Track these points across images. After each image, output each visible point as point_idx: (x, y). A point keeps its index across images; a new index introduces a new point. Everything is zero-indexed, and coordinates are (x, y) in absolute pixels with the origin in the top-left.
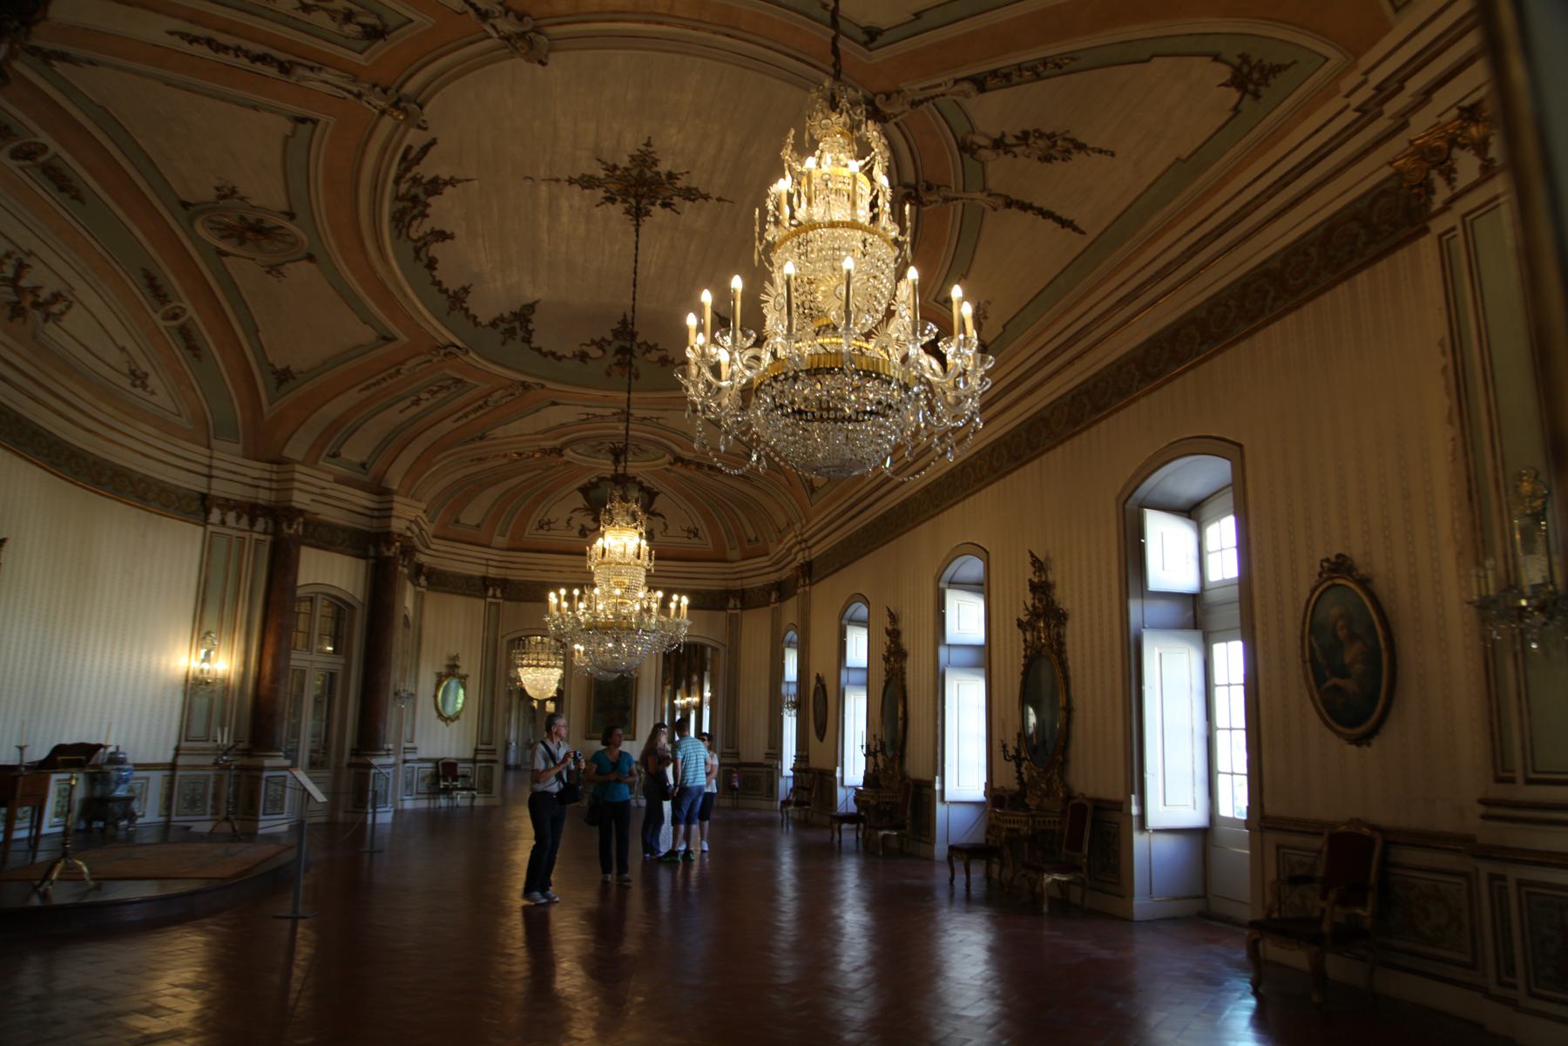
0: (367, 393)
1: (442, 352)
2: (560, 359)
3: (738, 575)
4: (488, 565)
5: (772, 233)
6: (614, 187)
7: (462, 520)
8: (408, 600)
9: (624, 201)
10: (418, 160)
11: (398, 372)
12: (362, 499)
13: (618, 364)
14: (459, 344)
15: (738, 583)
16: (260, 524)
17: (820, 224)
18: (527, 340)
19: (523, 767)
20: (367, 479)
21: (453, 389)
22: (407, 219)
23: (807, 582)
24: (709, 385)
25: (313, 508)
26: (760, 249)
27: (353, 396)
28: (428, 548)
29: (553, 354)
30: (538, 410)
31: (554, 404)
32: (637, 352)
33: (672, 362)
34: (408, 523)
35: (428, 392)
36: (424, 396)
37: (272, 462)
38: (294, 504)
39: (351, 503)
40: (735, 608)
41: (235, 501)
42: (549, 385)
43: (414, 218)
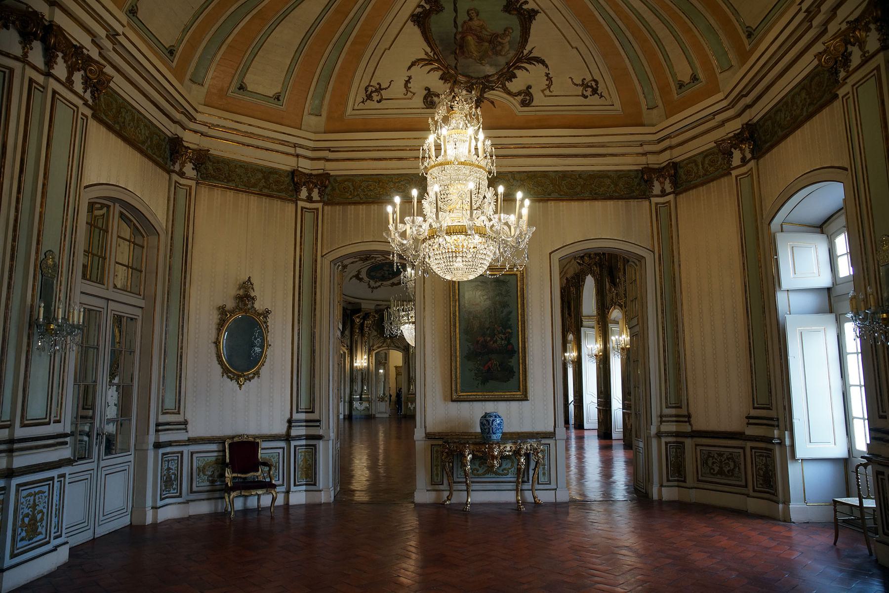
4: (298, 156)
15: (666, 157)
40: (663, 194)
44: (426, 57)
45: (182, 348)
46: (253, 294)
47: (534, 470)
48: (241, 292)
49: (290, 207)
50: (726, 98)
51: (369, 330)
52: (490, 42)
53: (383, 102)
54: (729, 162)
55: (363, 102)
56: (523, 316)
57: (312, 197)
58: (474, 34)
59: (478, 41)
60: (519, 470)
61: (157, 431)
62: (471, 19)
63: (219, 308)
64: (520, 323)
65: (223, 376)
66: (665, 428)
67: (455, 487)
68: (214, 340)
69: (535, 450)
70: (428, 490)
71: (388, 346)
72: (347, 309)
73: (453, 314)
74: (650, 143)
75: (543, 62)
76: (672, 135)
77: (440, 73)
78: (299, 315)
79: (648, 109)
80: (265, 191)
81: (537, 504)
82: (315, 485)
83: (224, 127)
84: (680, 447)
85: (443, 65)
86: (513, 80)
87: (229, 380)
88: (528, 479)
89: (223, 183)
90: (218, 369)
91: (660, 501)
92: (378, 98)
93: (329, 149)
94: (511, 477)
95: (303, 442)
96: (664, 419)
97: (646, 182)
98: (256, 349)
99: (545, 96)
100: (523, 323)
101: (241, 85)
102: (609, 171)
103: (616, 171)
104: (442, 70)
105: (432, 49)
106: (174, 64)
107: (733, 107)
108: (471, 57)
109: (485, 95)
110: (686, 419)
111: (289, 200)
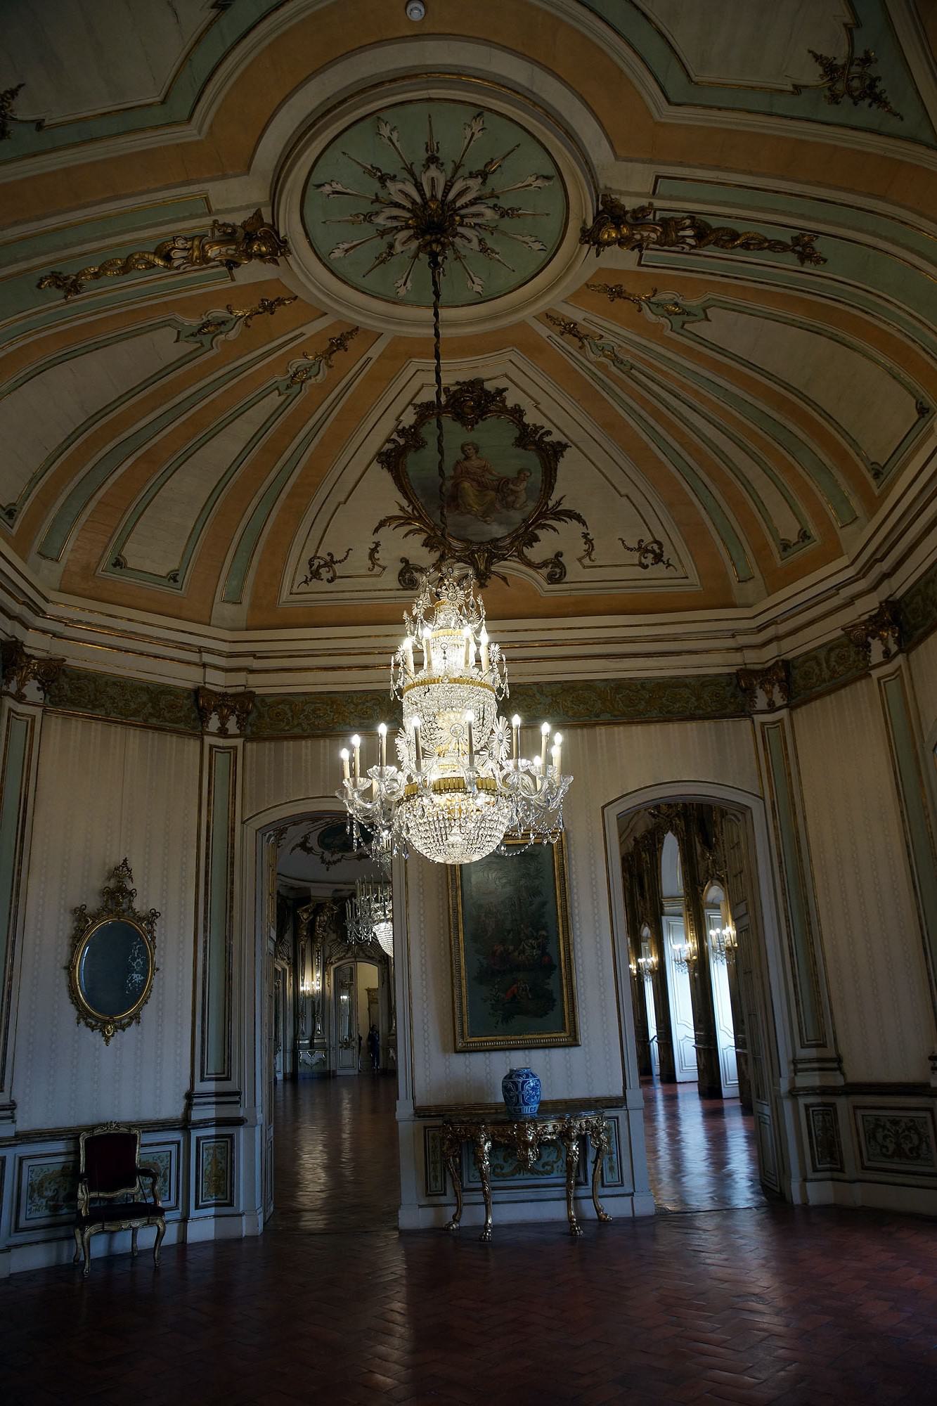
3: (770, 632)
4: (204, 666)
7: (134, 554)
40: (772, 708)
44: (401, 514)
45: (11, 979)
46: (130, 887)
47: (595, 1162)
48: (112, 884)
49: (192, 746)
50: (852, 563)
51: (324, 931)
52: (497, 490)
53: (337, 581)
54: (866, 658)
55: (306, 582)
56: (565, 908)
57: (227, 729)
58: (473, 480)
59: (479, 489)
60: (569, 1164)
62: (467, 458)
63: (75, 911)
64: (560, 921)
65: (78, 1023)
67: (466, 1198)
68: (65, 963)
69: (594, 1129)
70: (421, 1206)
71: (355, 957)
72: (287, 898)
73: (453, 910)
75: (578, 518)
76: (779, 620)
77: (424, 536)
78: (205, 918)
79: (739, 582)
80: (153, 721)
81: (602, 1222)
82: (231, 1204)
83: (88, 624)
84: (829, 1111)
85: (427, 525)
86: (534, 544)
87: (89, 1030)
88: (586, 1179)
89: (85, 710)
90: (72, 1011)
91: (805, 1206)
92: (329, 576)
93: (254, 655)
94: (557, 1177)
95: (212, 1131)
96: (800, 1066)
97: (744, 691)
98: (135, 975)
99: (584, 567)
100: (566, 919)
101: (118, 560)
102: (687, 677)
103: (698, 676)
104: (426, 532)
105: (410, 502)
106: (14, 531)
107: (864, 576)
108: (469, 513)
109: (493, 568)
110: (835, 1065)
111: (191, 734)
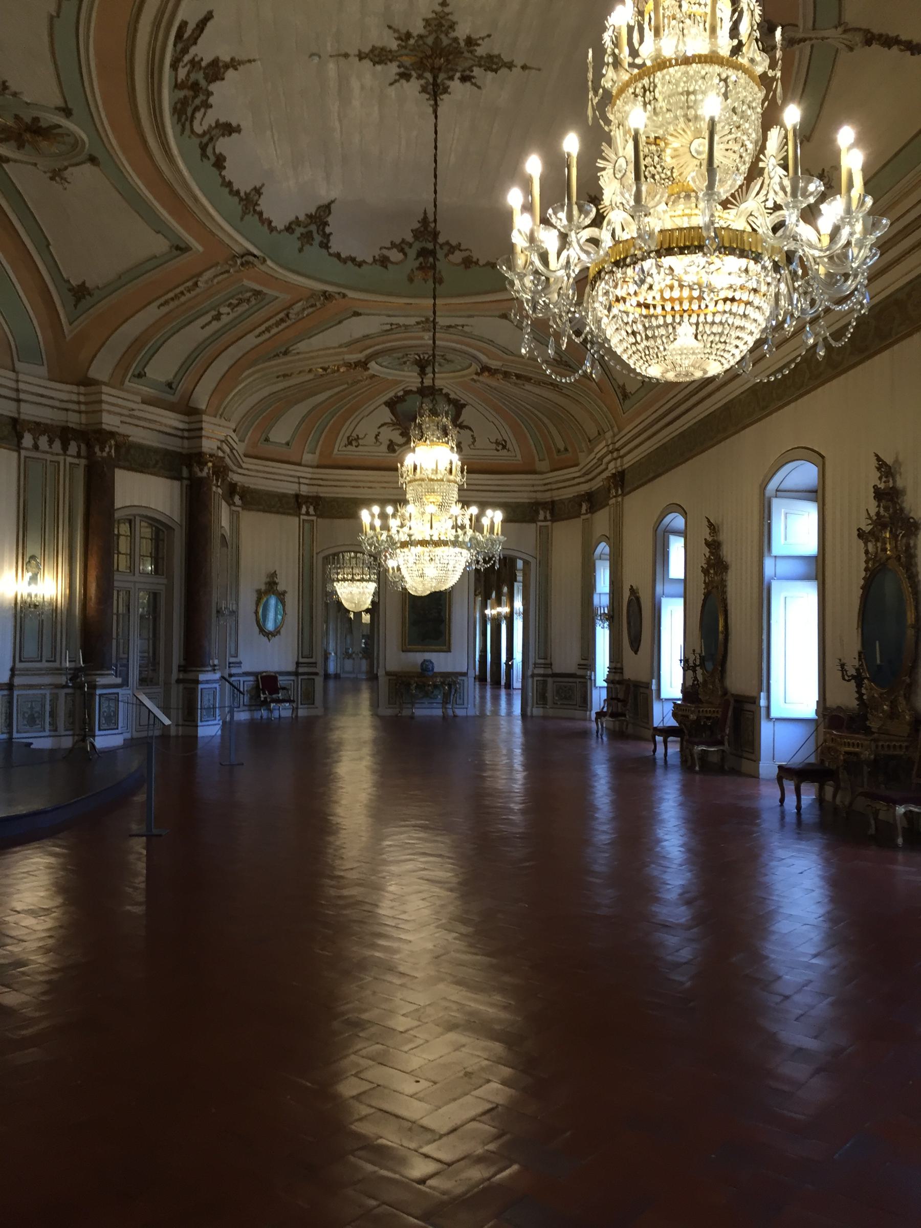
0: (165, 309)
1: (239, 262)
2: (360, 265)
3: (549, 487)
4: (299, 483)
5: (611, 78)
6: (407, 61)
7: (272, 438)
8: (223, 516)
9: (419, 77)
10: (194, 40)
11: (196, 284)
12: (172, 420)
13: (421, 268)
14: (256, 252)
15: (548, 494)
16: (73, 448)
17: (670, 60)
18: (325, 245)
19: (342, 676)
20: (174, 399)
21: (253, 302)
22: (189, 110)
23: (620, 492)
24: (536, 272)
25: (124, 429)
26: (596, 101)
27: (152, 313)
28: (241, 467)
29: (353, 260)
30: (340, 322)
31: (357, 314)
32: (440, 254)
33: (477, 263)
34: (219, 444)
35: (230, 305)
36: (224, 310)
37: (78, 384)
38: (104, 426)
39: (161, 424)
40: (545, 520)
41: (46, 425)
42: (351, 294)
43: (197, 109)
48: (268, 580)
53: (360, 447)
61: (229, 667)
66: (537, 671)
74: (538, 485)
75: (470, 429)
77: (400, 431)
80: (281, 510)
81: (455, 716)
84: (545, 683)
91: (532, 716)
92: (356, 444)
93: (322, 479)
103: (515, 503)
